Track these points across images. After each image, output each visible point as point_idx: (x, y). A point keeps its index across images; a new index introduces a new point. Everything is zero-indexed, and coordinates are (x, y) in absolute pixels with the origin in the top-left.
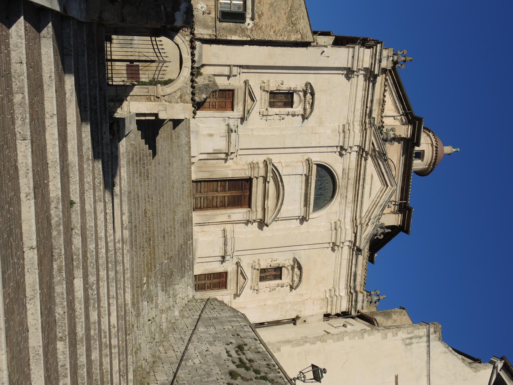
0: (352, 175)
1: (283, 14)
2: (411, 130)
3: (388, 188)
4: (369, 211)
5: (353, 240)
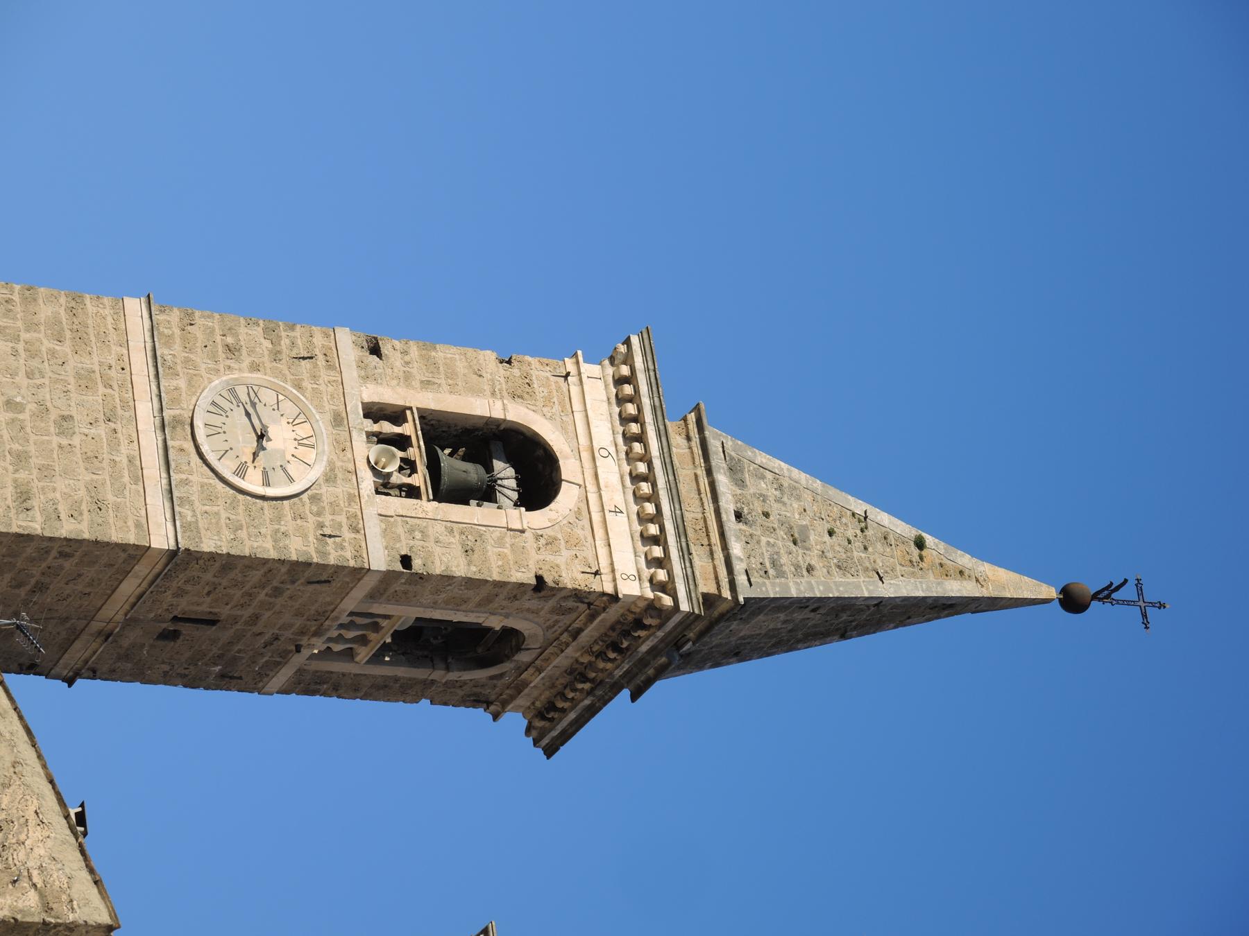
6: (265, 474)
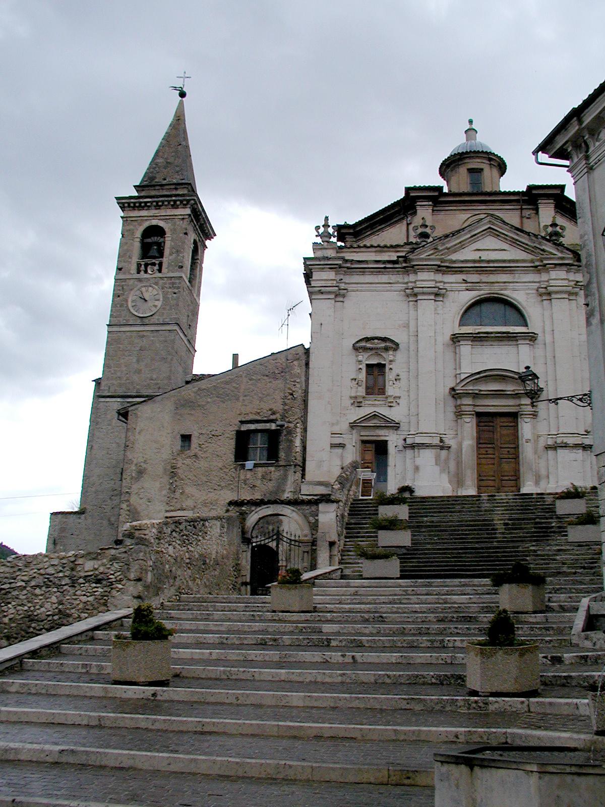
0: (474, 278)
1: (271, 384)
2: (422, 201)
3: (492, 226)
4: (525, 248)
5: (565, 268)
6: (156, 300)
